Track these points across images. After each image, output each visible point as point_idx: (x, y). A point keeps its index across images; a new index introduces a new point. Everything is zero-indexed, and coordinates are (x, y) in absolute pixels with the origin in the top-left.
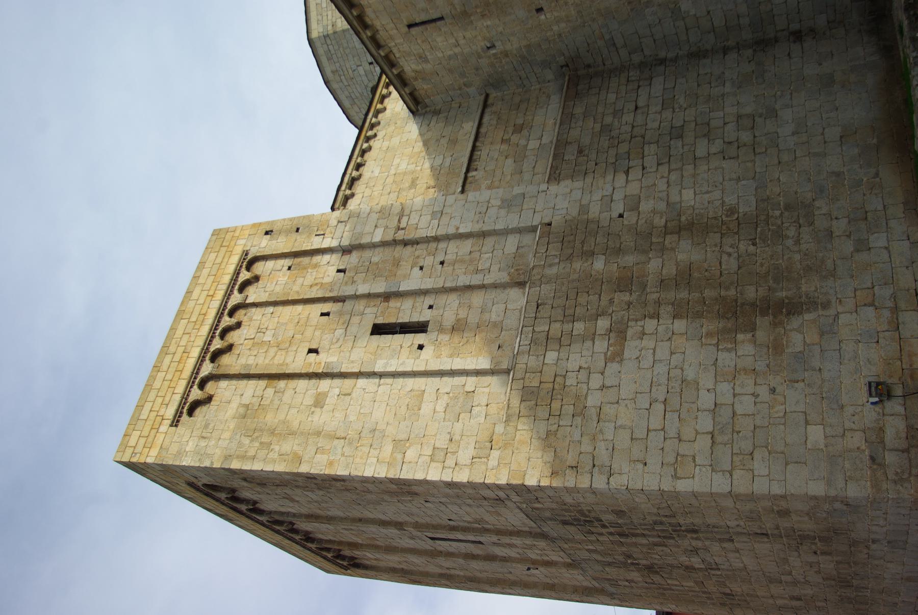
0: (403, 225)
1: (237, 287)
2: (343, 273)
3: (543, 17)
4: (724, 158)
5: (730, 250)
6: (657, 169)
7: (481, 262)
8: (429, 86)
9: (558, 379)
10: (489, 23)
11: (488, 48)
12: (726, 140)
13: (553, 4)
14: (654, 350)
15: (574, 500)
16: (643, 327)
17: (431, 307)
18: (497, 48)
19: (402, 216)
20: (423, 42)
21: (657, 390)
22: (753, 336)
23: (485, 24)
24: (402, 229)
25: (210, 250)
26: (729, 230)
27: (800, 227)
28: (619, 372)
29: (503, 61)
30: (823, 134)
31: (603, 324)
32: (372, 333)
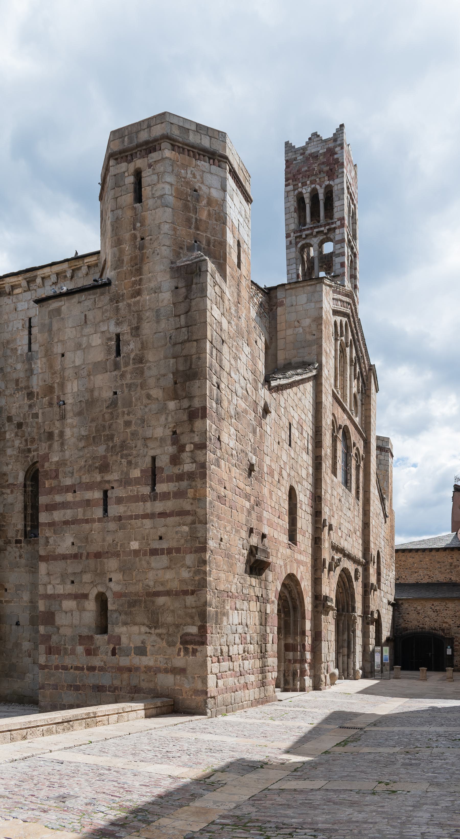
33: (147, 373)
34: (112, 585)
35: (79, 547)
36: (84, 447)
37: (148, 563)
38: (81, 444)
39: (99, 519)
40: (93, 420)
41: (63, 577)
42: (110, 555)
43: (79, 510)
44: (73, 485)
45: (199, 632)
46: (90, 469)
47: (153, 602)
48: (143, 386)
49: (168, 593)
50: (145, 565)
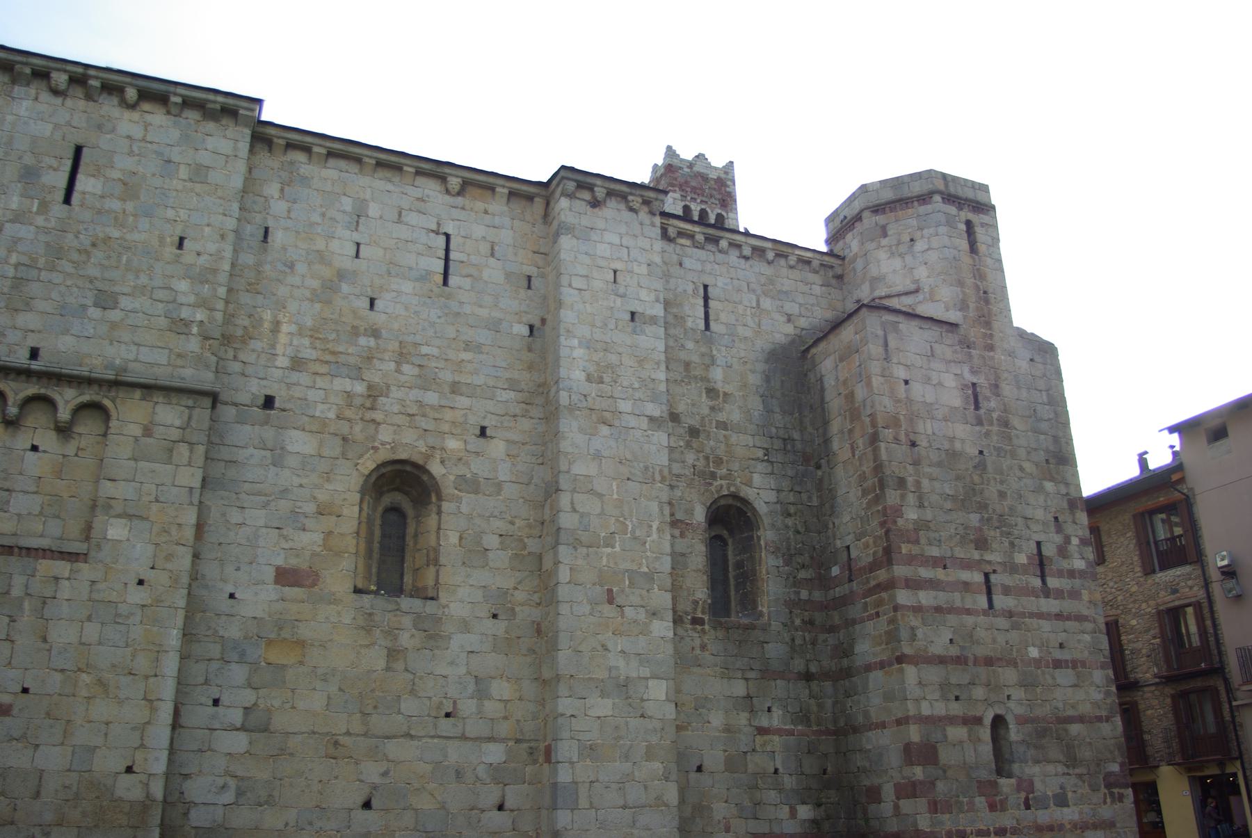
33: (1015, 441)
34: (1011, 704)
35: (962, 648)
36: (950, 510)
37: (1054, 678)
38: (948, 505)
39: (984, 610)
40: (958, 478)
41: (944, 686)
42: (1005, 664)
43: (956, 594)
44: (943, 558)
45: (1122, 771)
46: (963, 541)
47: (1066, 730)
48: (1013, 455)
49: (1081, 719)
50: (1050, 681)
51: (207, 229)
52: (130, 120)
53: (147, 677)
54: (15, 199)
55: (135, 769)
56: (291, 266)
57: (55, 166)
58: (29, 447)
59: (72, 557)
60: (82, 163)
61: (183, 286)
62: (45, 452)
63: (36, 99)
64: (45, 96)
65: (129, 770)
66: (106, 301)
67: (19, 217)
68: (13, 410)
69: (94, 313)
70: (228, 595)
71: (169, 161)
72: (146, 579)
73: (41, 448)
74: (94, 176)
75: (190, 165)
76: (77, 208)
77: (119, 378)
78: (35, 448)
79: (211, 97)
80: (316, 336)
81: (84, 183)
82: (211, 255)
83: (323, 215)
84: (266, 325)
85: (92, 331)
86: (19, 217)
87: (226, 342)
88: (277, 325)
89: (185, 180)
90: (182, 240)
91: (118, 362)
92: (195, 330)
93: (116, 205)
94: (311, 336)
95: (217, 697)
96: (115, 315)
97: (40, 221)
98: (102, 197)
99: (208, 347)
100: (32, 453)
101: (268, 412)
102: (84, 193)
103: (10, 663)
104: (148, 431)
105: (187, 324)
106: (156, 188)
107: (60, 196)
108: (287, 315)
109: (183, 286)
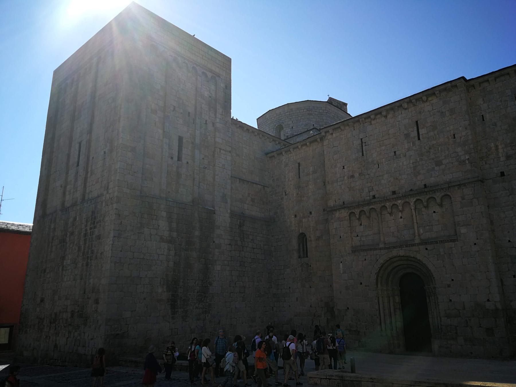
0: (222, 151)
1: (205, 71)
2: (205, 123)
3: (293, 217)
4: (230, 281)
5: (196, 283)
6: (230, 256)
7: (203, 184)
8: (276, 164)
9: (155, 217)
10: (295, 195)
11: (286, 193)
12: (237, 283)
13: (297, 222)
14: (163, 254)
15: (107, 221)
16: (172, 250)
17: (187, 163)
18: (285, 196)
19: (225, 151)
20: (292, 167)
21: (148, 256)
22: (165, 291)
23: (294, 194)
24: (220, 151)
25: (222, 57)
26: (204, 283)
27: (202, 309)
28: (156, 241)
29: (280, 197)
30: (234, 318)
31: (175, 234)
32: (179, 136)
51: (460, 128)
52: (427, 106)
53: (485, 272)
54: (406, 145)
55: (490, 300)
56: (495, 125)
57: (413, 130)
58: (433, 212)
59: (453, 241)
60: (419, 126)
61: (459, 149)
62: (437, 212)
63: (401, 113)
64: (403, 112)
65: (488, 300)
66: (438, 163)
67: (409, 150)
68: (425, 204)
69: (437, 168)
70: (508, 241)
71: (442, 112)
72: (476, 243)
73: (436, 212)
74: (423, 128)
75: (448, 110)
76: (422, 140)
77: (449, 185)
78: (434, 212)
79: (446, 85)
80: (512, 145)
81: (422, 131)
82: (464, 136)
83: (501, 101)
84: (493, 148)
85: (438, 174)
86: (409, 150)
87: (481, 160)
88: (497, 146)
89: (448, 116)
90: (454, 135)
91: (448, 180)
92: (467, 162)
93: (432, 134)
94: (510, 146)
95: (514, 275)
96: (443, 167)
97: (414, 148)
98: (427, 133)
99: (473, 166)
100: (434, 214)
101: (503, 177)
102: (422, 134)
103: (446, 273)
104: (463, 198)
105: (464, 161)
106: (441, 123)
107: (417, 138)
108: (499, 142)
109: (459, 149)
